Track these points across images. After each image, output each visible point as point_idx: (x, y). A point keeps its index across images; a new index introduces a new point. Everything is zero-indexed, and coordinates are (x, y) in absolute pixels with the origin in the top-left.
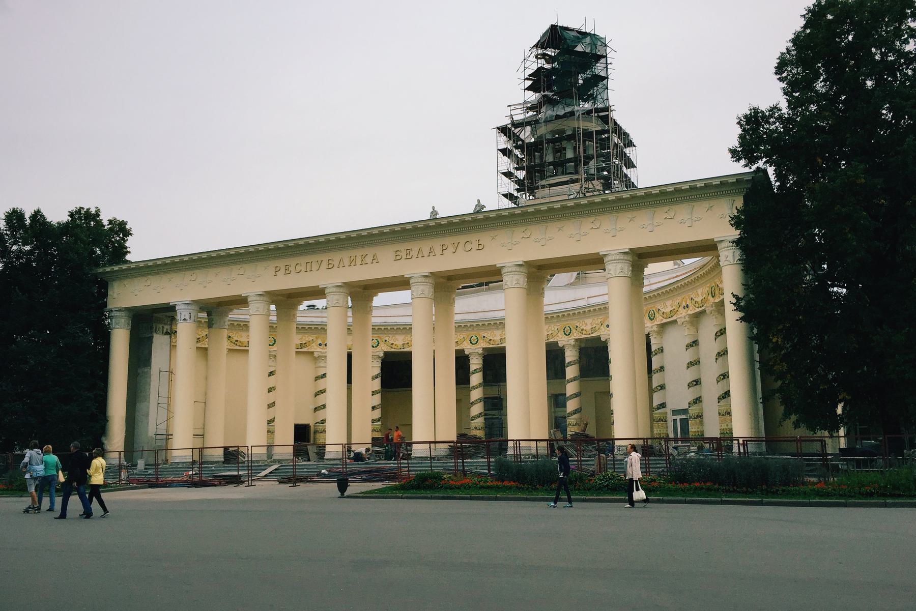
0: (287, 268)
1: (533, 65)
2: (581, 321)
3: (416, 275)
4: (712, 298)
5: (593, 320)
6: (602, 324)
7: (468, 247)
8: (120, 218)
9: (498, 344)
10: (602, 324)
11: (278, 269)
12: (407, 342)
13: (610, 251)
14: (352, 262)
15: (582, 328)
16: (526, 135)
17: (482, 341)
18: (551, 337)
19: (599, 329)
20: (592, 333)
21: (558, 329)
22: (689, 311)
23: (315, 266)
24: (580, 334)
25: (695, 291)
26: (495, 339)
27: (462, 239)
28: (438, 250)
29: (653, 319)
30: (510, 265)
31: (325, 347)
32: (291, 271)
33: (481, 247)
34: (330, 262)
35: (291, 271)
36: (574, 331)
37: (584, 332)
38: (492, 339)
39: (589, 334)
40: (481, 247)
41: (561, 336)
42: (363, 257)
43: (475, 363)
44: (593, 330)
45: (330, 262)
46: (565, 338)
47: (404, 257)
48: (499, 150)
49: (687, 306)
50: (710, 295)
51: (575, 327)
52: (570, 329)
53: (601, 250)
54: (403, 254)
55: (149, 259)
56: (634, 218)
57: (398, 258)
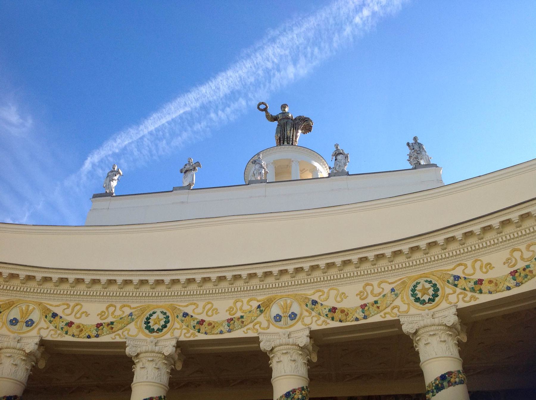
2: (469, 263)
9: (221, 332)
15: (478, 276)
17: (177, 325)
18: (373, 309)
21: (393, 290)
24: (470, 294)
37: (485, 287)
38: (207, 319)
41: (404, 308)
46: (415, 309)
51: (451, 279)
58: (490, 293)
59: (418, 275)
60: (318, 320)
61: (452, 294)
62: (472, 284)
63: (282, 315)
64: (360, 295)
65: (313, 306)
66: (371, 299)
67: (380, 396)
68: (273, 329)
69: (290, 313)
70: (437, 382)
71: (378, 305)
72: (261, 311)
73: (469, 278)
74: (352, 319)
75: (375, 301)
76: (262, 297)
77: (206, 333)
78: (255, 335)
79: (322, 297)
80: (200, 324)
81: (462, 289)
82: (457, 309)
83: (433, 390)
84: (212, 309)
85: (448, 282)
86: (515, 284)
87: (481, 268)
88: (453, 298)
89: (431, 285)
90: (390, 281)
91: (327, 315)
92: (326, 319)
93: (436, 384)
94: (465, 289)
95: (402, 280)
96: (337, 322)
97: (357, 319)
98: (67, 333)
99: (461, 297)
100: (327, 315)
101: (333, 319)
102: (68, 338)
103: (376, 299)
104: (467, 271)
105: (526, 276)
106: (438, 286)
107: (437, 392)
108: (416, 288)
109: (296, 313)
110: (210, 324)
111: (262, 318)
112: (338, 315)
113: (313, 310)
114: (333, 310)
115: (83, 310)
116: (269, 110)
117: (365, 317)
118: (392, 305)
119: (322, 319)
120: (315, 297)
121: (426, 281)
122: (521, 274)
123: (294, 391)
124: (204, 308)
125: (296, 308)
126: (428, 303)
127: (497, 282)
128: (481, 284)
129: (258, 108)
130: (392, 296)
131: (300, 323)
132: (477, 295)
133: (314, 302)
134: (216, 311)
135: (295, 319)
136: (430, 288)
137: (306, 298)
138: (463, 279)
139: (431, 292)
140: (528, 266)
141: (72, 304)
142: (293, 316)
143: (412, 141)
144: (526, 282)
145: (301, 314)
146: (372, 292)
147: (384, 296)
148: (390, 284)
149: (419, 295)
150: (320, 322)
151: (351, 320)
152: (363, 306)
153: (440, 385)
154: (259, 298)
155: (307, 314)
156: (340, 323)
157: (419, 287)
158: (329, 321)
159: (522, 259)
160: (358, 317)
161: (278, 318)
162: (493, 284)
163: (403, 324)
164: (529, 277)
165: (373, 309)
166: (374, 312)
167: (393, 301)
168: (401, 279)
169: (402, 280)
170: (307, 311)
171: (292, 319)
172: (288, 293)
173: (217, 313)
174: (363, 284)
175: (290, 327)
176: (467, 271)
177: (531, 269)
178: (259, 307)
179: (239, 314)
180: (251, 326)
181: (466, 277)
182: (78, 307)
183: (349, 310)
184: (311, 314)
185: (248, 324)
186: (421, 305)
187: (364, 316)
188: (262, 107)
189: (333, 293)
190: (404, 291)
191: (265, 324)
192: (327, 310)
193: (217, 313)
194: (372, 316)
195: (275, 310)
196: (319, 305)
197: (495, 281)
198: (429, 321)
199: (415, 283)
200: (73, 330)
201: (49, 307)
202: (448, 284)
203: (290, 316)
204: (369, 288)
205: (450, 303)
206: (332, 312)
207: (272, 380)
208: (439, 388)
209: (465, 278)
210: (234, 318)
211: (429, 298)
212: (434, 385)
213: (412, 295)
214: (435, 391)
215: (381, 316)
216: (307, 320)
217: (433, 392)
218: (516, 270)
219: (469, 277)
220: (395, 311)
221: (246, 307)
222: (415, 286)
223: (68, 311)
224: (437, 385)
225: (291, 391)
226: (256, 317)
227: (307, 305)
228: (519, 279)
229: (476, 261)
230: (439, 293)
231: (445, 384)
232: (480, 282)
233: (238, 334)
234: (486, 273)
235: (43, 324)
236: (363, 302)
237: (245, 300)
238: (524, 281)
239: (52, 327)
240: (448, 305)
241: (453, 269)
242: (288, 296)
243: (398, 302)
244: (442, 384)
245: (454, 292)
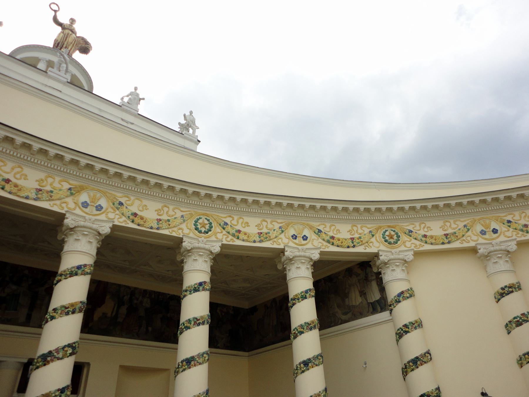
2: (236, 218)
5: (264, 221)
9: (27, 198)
19: (276, 237)
21: (182, 216)
24: (231, 237)
26: (20, 182)
36: (217, 229)
39: (255, 242)
46: (194, 234)
51: (222, 223)
52: (210, 224)
58: (243, 240)
59: (202, 213)
60: (121, 218)
61: (220, 233)
62: (233, 231)
63: (90, 204)
64: (158, 211)
65: (119, 206)
67: (107, 283)
68: (78, 211)
69: (97, 204)
70: (196, 286)
71: (170, 223)
72: (72, 194)
73: (233, 227)
74: (148, 226)
75: (168, 219)
76: (75, 183)
77: (10, 193)
79: (128, 202)
80: (6, 182)
81: (227, 232)
82: (222, 244)
83: (191, 290)
84: (22, 173)
85: (220, 225)
86: (259, 240)
87: (242, 223)
88: (220, 236)
89: (208, 222)
90: (182, 209)
91: (129, 217)
92: (126, 219)
93: (195, 287)
94: (229, 233)
95: (190, 212)
96: (135, 225)
97: (151, 228)
99: (225, 237)
100: (129, 217)
101: (133, 222)
103: (169, 218)
104: (233, 222)
105: (267, 238)
106: (213, 225)
107: (194, 292)
108: (198, 221)
109: (102, 205)
111: (69, 200)
112: (137, 220)
113: (118, 209)
114: (135, 215)
116: (58, 14)
118: (179, 227)
120: (123, 200)
121: (206, 219)
122: (264, 236)
123: (85, 266)
126: (203, 233)
127: (250, 235)
128: (240, 233)
129: (50, 6)
130: (180, 220)
131: (104, 215)
132: (235, 239)
133: (121, 204)
135: (100, 211)
136: (207, 224)
137: (115, 198)
138: (230, 226)
139: (207, 227)
140: (269, 233)
143: (188, 114)
144: (265, 241)
145: (107, 209)
146: (167, 212)
147: (175, 218)
148: (181, 211)
149: (199, 226)
150: (121, 220)
151: (147, 227)
152: (159, 220)
153: (197, 288)
155: (110, 210)
156: (137, 226)
157: (200, 221)
159: (267, 227)
160: (153, 226)
161: (85, 205)
162: (246, 236)
163: (185, 242)
164: (267, 239)
165: (165, 225)
166: (165, 227)
167: (181, 224)
168: (190, 211)
169: (190, 212)
170: (112, 208)
171: (97, 210)
172: (99, 188)
176: (233, 222)
177: (270, 235)
178: (70, 189)
179: (48, 188)
180: (58, 202)
181: (232, 225)
183: (147, 218)
184: (116, 211)
185: (56, 200)
186: (198, 233)
187: (158, 227)
188: (55, 7)
189: (137, 202)
190: (190, 220)
192: (130, 213)
194: (164, 229)
195: (84, 197)
196: (125, 207)
197: (248, 234)
198: (201, 245)
199: (198, 217)
202: (219, 226)
203: (96, 207)
204: (166, 209)
205: (217, 238)
206: (134, 216)
207: (63, 253)
208: (196, 290)
209: (231, 226)
210: (43, 189)
211: (205, 230)
212: (193, 287)
213: (194, 225)
214: (192, 291)
215: (169, 231)
216: (111, 216)
217: (190, 292)
218: (262, 233)
219: (234, 226)
220: (180, 231)
222: (198, 219)
224: (195, 288)
225: (83, 265)
226: (65, 197)
227: (114, 204)
228: (262, 238)
229: (241, 218)
230: (213, 229)
231: (201, 288)
232: (239, 231)
234: (244, 227)
236: (159, 217)
238: (264, 240)
240: (216, 239)
241: (225, 218)
242: (99, 191)
243: (183, 226)
244: (199, 288)
245: (222, 232)
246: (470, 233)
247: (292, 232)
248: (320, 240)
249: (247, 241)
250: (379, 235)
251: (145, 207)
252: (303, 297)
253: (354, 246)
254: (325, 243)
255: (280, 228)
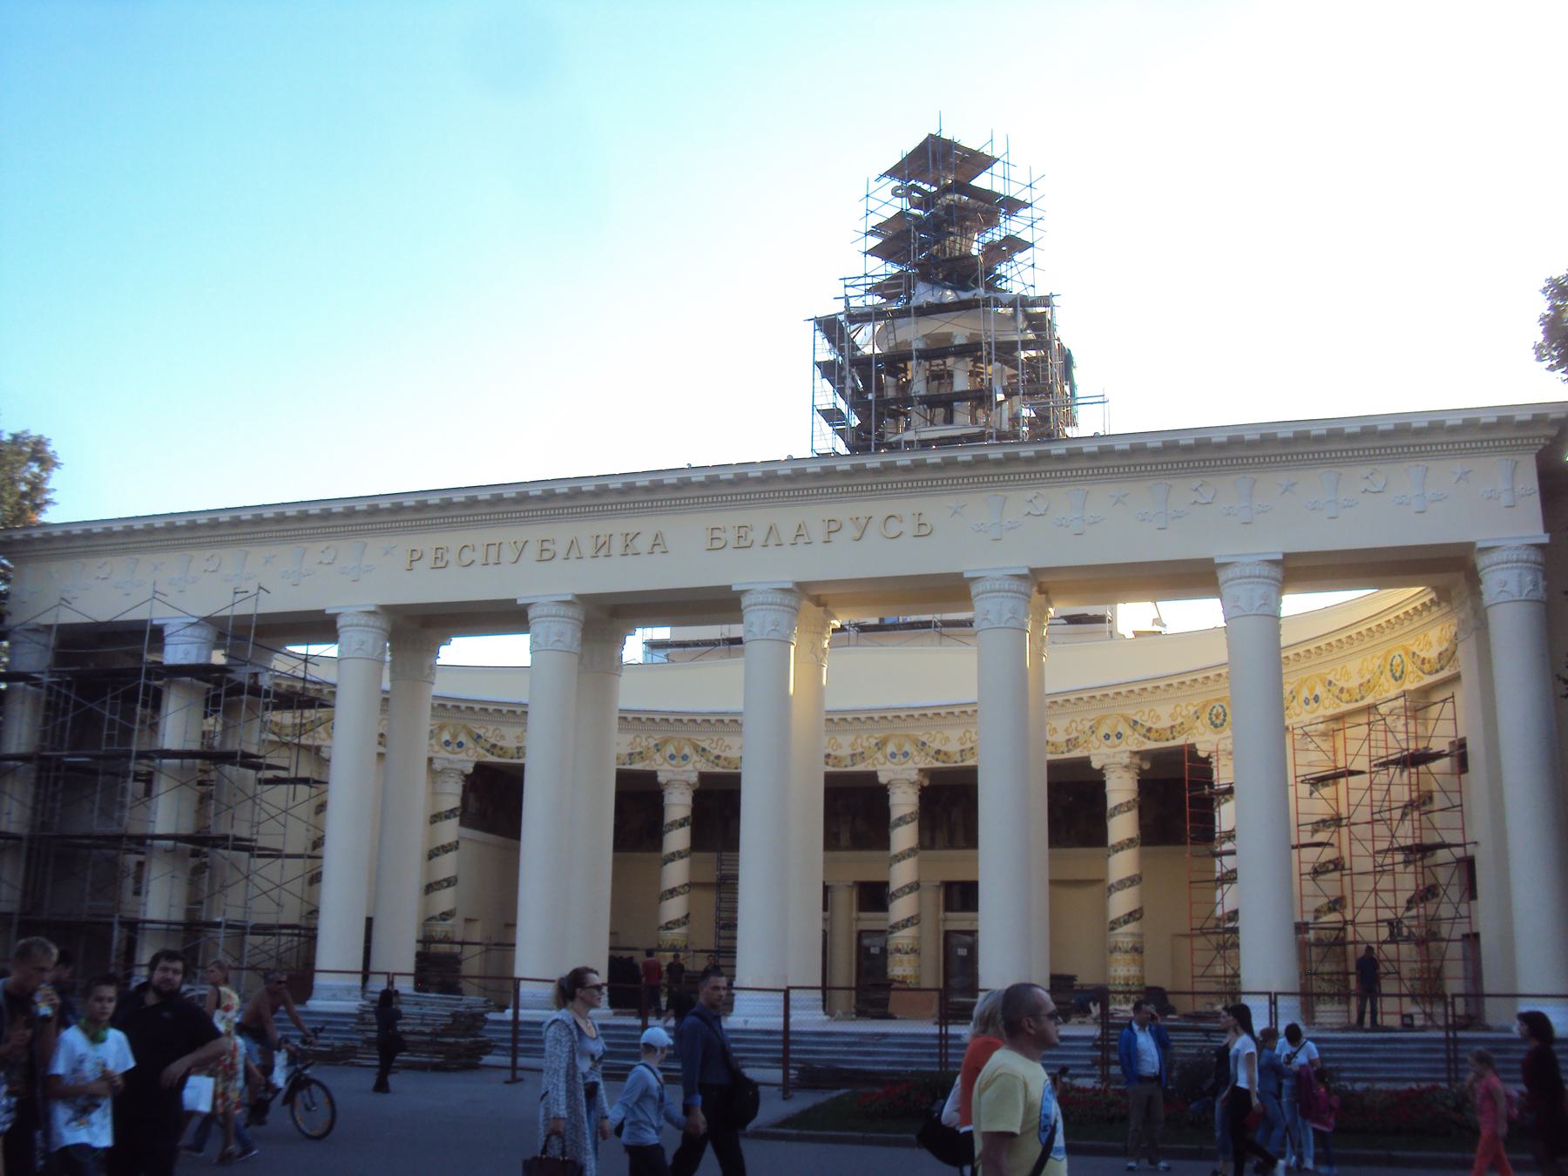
0: (439, 556)
1: (889, 205)
3: (759, 587)
4: (1392, 681)
6: (1093, 732)
7: (894, 528)
8: (35, 432)
9: (846, 766)
10: (1093, 732)
11: (417, 556)
12: (638, 750)
13: (1238, 555)
14: (602, 547)
16: (865, 339)
18: (969, 754)
19: (1085, 742)
20: (1069, 751)
22: (1321, 707)
23: (508, 554)
25: (1339, 668)
26: (839, 753)
27: (878, 508)
28: (817, 531)
29: (1222, 725)
30: (997, 574)
31: (457, 750)
32: (447, 562)
33: (924, 531)
34: (546, 545)
35: (447, 562)
38: (833, 753)
39: (1063, 753)
40: (924, 531)
42: (630, 537)
43: (678, 805)
44: (1071, 743)
45: (546, 545)
47: (733, 541)
48: (818, 364)
49: (1316, 699)
50: (1389, 675)
53: (1218, 554)
54: (731, 536)
55: (116, 517)
56: (1293, 485)
57: (717, 544)
66: (968, 745)
68: (889, 766)
72: (879, 749)
76: (879, 735)
77: (833, 766)
78: (874, 769)
97: (956, 762)
98: (717, 765)
101: (937, 760)
102: (718, 770)
110: (836, 758)
111: (879, 755)
114: (938, 752)
115: (726, 743)
117: (962, 761)
119: (929, 759)
120: (924, 739)
124: (829, 742)
125: (908, 747)
134: (840, 746)
141: (715, 738)
142: (906, 754)
150: (927, 761)
152: (962, 751)
154: (877, 736)
158: (934, 761)
165: (969, 754)
173: (841, 747)
174: (964, 730)
175: (902, 764)
178: (877, 744)
179: (860, 750)
180: (870, 761)
182: (720, 743)
191: (882, 760)
193: (841, 747)
195: (890, 748)
200: (721, 762)
201: (698, 743)
221: (866, 744)
223: (714, 745)
233: (860, 767)
235: (695, 757)
236: (962, 747)
237: (865, 737)
239: (704, 760)
246: (1295, 702)
247: (1104, 730)
248: (1136, 735)
249: (1056, 753)
250: (1205, 718)
251: (947, 739)
252: (1119, 809)
253: (1174, 738)
254: (1142, 739)
255: (1091, 727)
